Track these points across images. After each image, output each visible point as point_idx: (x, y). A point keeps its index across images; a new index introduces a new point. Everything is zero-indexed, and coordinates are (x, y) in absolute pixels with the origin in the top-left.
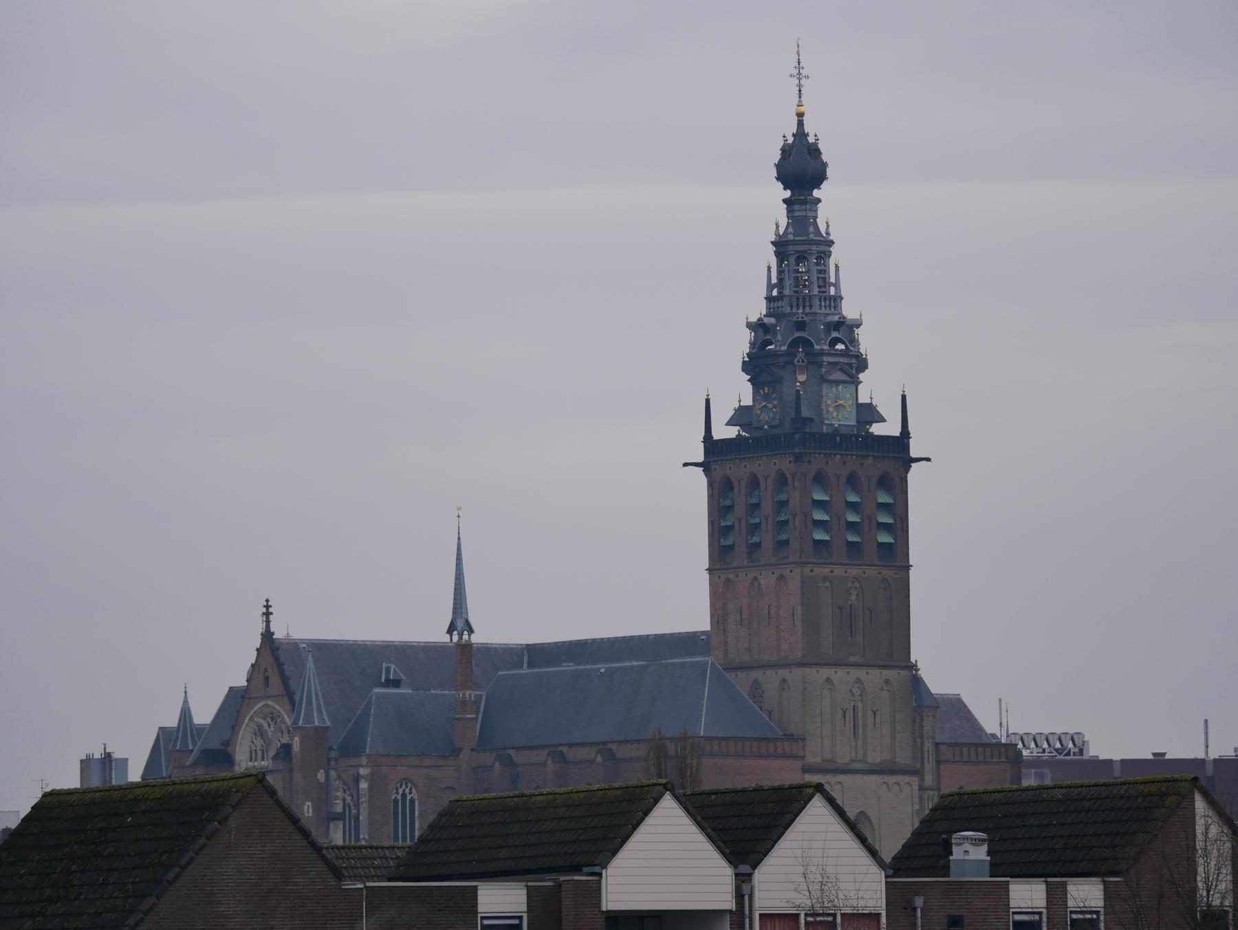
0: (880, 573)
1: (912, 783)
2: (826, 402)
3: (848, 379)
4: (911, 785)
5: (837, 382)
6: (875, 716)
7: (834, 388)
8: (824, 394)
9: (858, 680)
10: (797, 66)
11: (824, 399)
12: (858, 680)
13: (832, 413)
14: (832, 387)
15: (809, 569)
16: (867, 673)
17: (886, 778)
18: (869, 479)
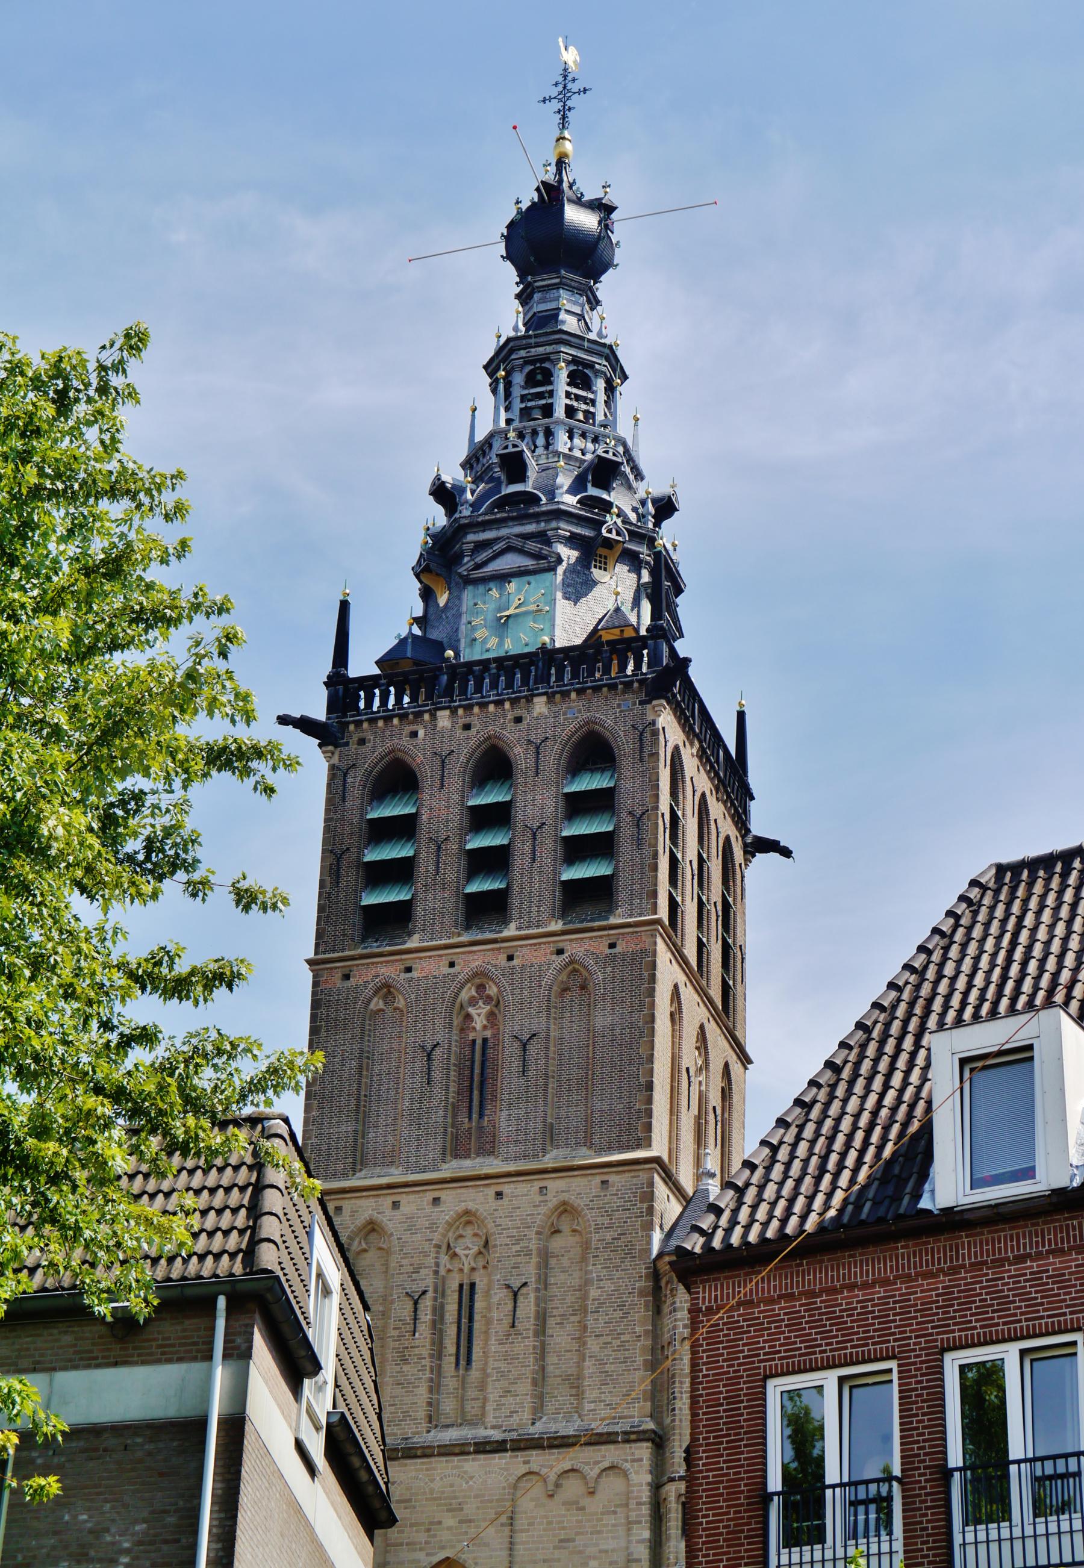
0: (560, 952)
1: (627, 1465)
2: (470, 623)
3: (529, 563)
4: (625, 1474)
5: (503, 578)
6: (515, 1302)
7: (495, 593)
8: (464, 609)
9: (468, 1217)
10: (561, 79)
11: (464, 620)
12: (468, 1217)
13: (485, 641)
14: (490, 590)
15: (338, 975)
16: (499, 1195)
17: (537, 1459)
18: (538, 748)
